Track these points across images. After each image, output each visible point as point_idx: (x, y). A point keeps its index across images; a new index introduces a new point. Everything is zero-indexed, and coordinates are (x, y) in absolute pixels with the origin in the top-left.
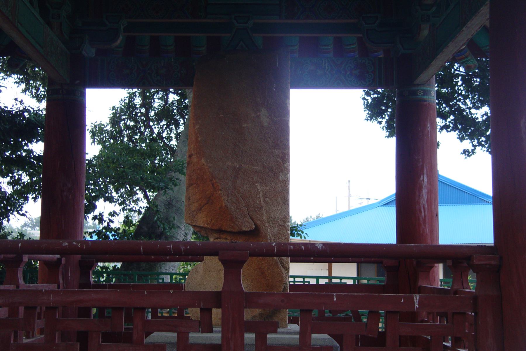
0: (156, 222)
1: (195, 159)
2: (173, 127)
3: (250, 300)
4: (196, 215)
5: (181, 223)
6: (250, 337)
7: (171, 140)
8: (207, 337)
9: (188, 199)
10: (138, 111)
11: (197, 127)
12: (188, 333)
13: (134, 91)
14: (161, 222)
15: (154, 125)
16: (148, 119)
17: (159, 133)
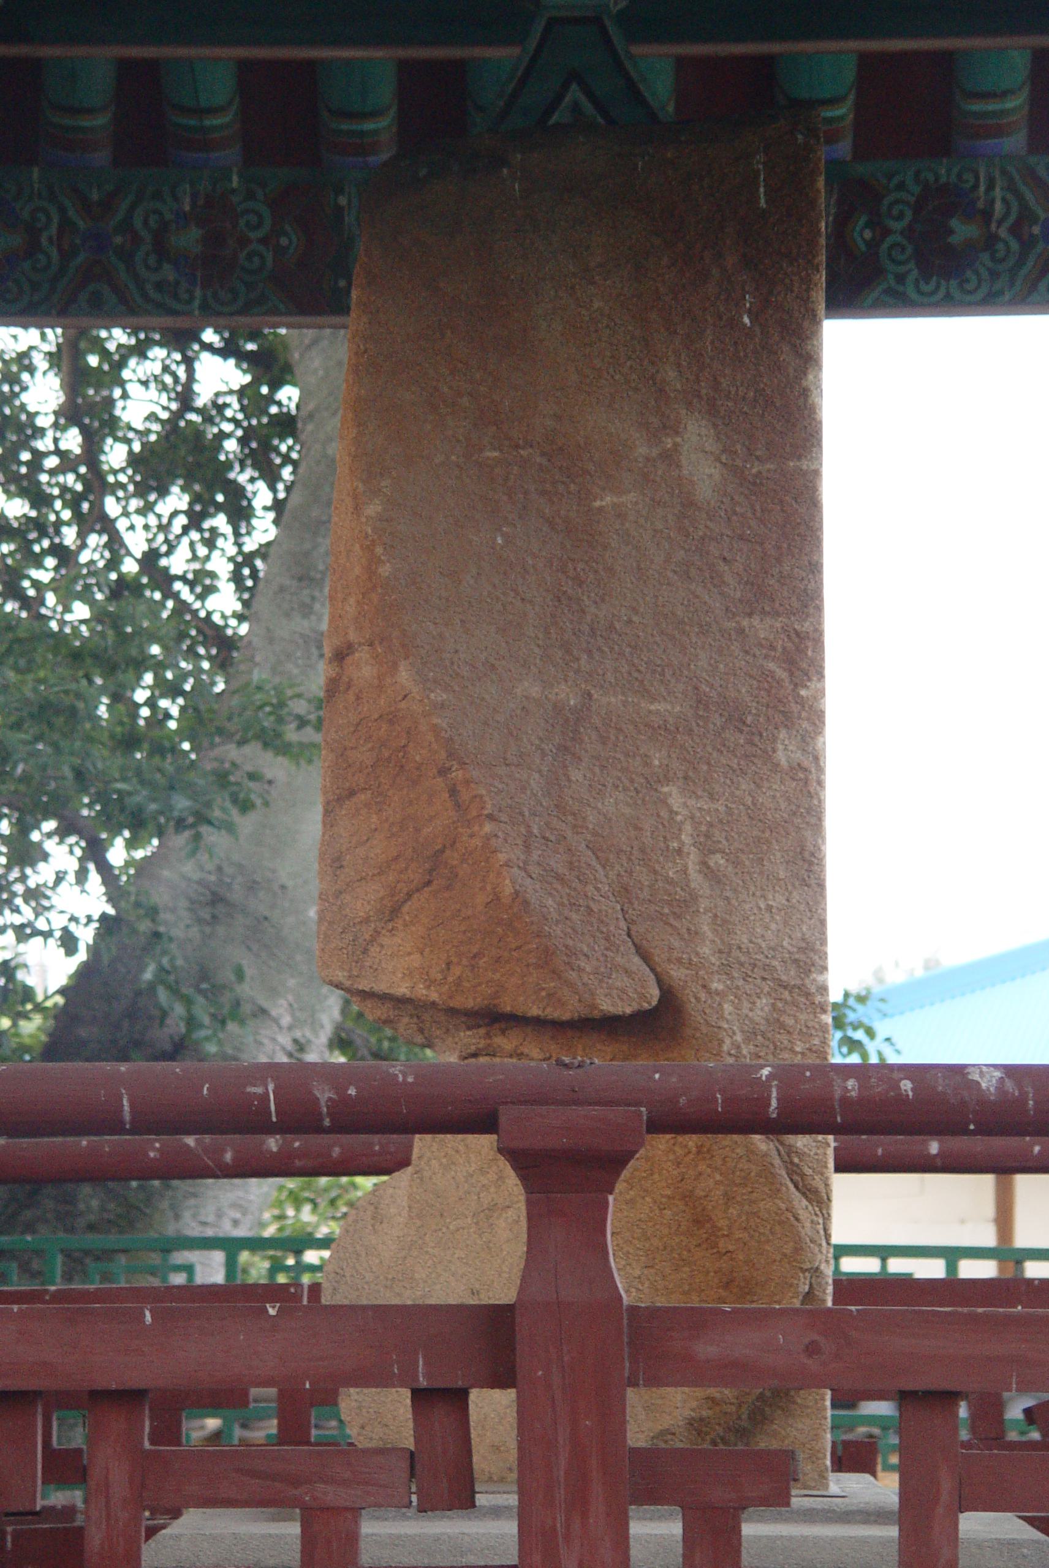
0: (152, 987)
1: (363, 669)
2: (220, 521)
3: (653, 1343)
4: (373, 940)
5: (273, 992)
6: (656, 1531)
7: (210, 590)
8: (437, 1539)
9: (333, 861)
10: (42, 445)
11: (373, 509)
12: (355, 1512)
13: (22, 347)
14: (174, 991)
15: (126, 514)
16: (97, 484)
17: (150, 559)
